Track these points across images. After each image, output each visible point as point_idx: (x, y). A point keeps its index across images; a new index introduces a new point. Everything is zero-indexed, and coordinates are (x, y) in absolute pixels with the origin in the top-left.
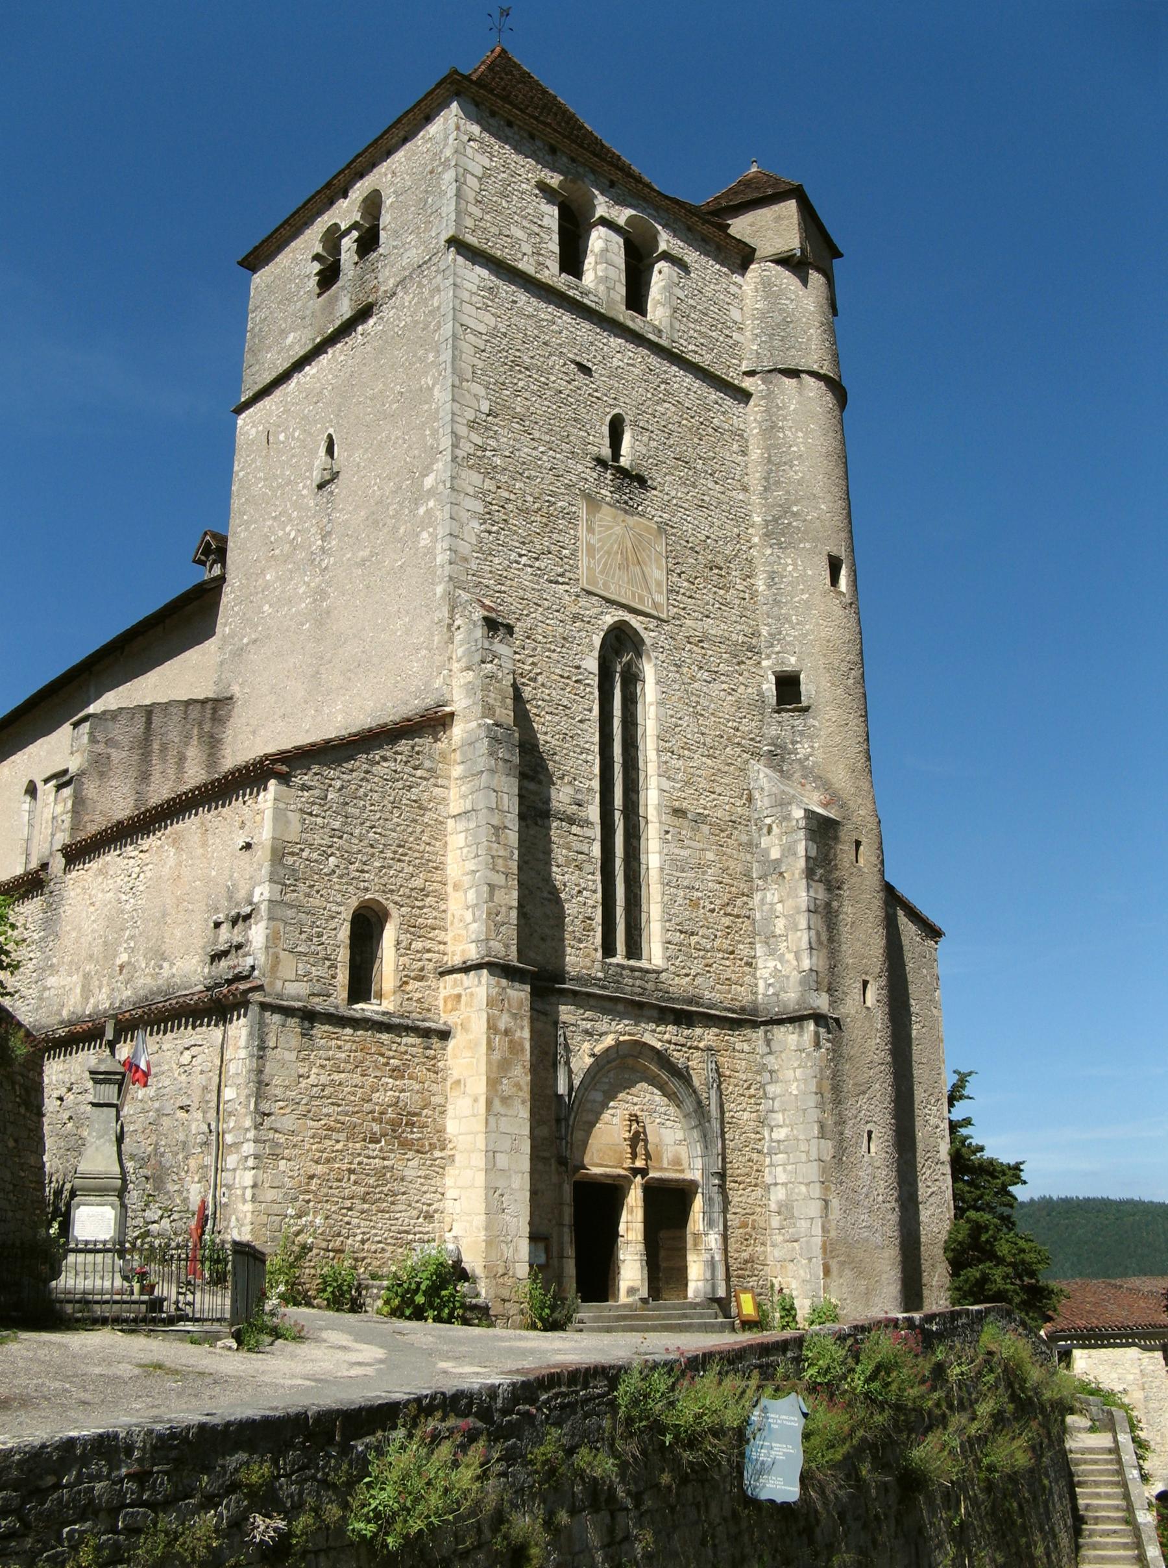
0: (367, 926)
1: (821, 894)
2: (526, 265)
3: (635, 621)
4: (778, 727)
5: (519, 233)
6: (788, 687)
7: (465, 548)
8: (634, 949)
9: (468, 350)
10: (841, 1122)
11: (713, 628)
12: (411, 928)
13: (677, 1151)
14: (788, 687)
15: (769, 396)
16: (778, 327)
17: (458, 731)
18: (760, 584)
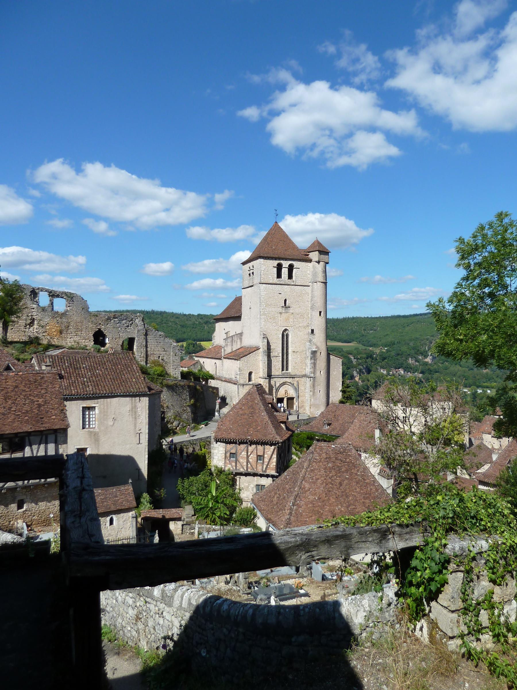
0: (250, 374)
1: (313, 361)
2: (271, 282)
3: (287, 328)
4: (311, 337)
5: (270, 276)
6: (312, 331)
7: (261, 326)
8: (287, 369)
9: (261, 298)
10: (314, 390)
11: (300, 325)
12: (256, 373)
13: (292, 393)
14: (312, 331)
15: (312, 286)
16: (315, 274)
17: (261, 350)
18: (310, 316)
